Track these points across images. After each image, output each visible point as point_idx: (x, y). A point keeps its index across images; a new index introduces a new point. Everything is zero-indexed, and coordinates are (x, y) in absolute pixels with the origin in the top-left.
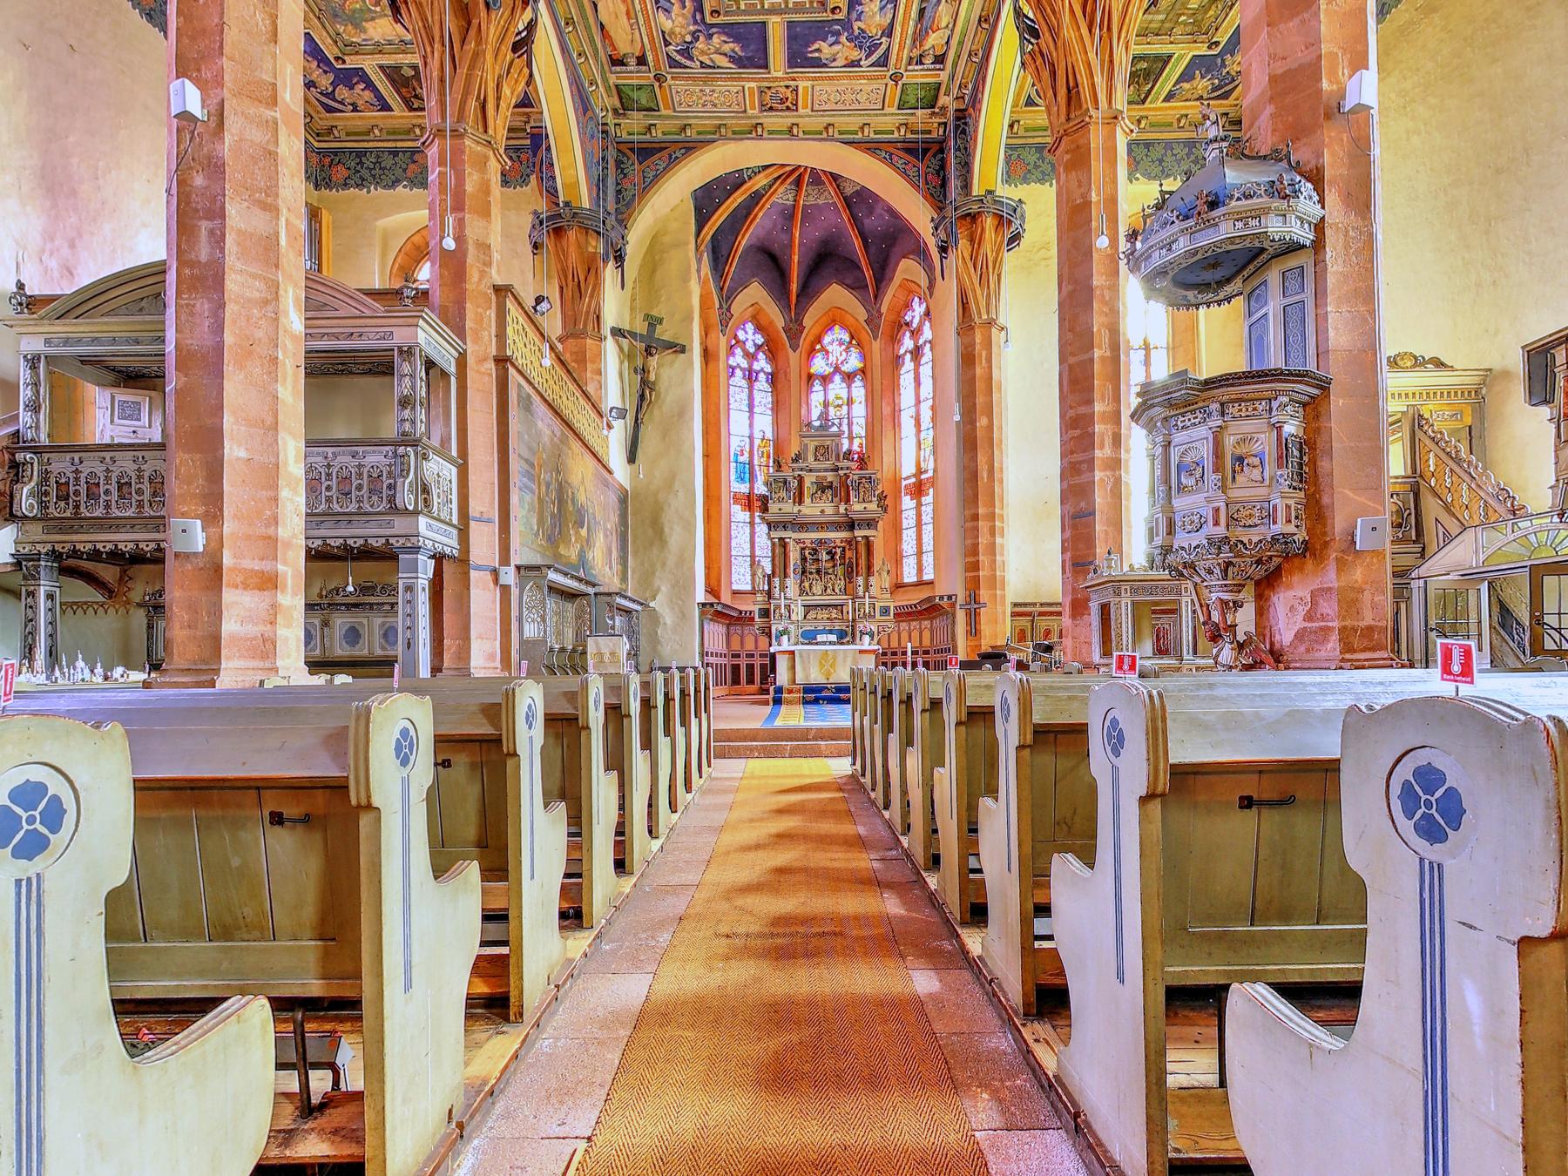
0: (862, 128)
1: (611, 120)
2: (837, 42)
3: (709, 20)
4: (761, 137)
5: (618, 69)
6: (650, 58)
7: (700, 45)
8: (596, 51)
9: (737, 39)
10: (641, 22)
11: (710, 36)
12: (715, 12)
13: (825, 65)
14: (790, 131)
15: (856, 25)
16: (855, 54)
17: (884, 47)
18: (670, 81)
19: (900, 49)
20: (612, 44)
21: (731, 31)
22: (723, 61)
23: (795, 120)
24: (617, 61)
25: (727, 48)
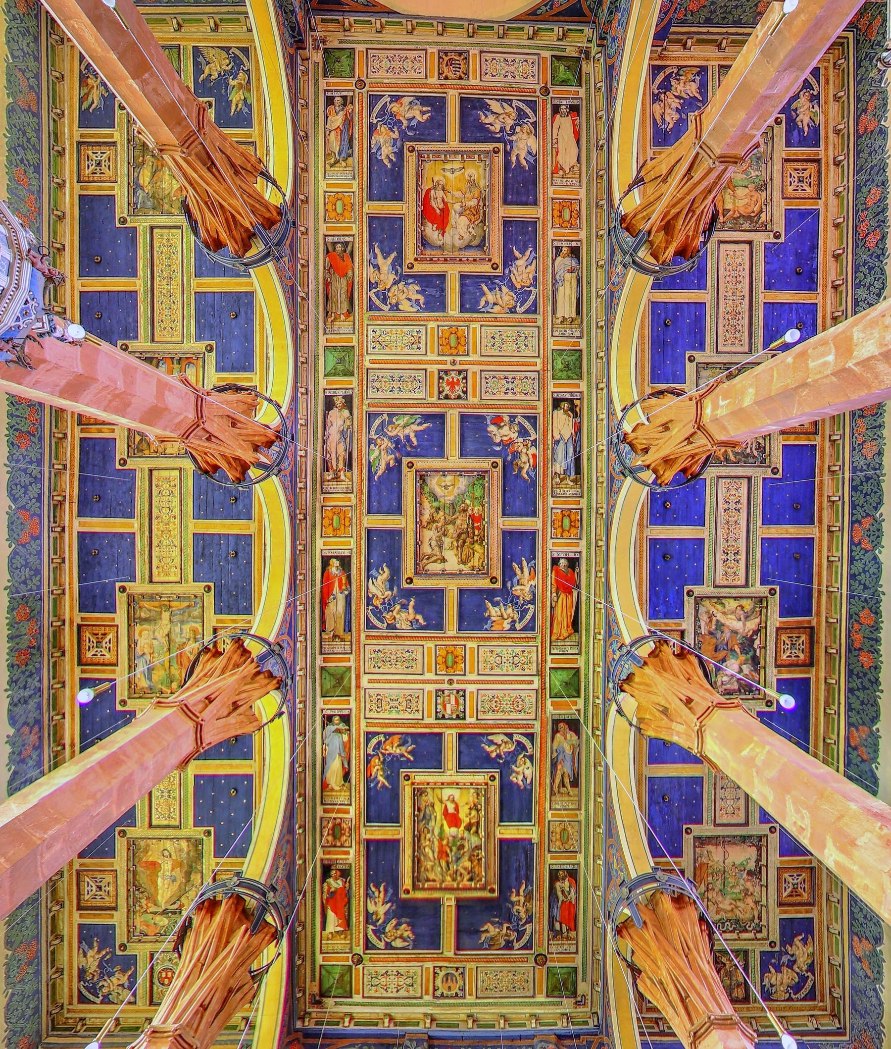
0: (382, 27)
1: (594, 50)
3: (501, 146)
4: (471, 21)
5: (575, 102)
6: (549, 112)
7: (510, 122)
8: (588, 121)
9: (482, 128)
11: (502, 130)
13: (417, 98)
14: (444, 27)
15: (396, 135)
16: (395, 107)
17: (374, 115)
18: (538, 87)
19: (360, 107)
20: (574, 125)
21: (486, 136)
22: (495, 106)
23: (440, 39)
24: (574, 109)
25: (491, 119)
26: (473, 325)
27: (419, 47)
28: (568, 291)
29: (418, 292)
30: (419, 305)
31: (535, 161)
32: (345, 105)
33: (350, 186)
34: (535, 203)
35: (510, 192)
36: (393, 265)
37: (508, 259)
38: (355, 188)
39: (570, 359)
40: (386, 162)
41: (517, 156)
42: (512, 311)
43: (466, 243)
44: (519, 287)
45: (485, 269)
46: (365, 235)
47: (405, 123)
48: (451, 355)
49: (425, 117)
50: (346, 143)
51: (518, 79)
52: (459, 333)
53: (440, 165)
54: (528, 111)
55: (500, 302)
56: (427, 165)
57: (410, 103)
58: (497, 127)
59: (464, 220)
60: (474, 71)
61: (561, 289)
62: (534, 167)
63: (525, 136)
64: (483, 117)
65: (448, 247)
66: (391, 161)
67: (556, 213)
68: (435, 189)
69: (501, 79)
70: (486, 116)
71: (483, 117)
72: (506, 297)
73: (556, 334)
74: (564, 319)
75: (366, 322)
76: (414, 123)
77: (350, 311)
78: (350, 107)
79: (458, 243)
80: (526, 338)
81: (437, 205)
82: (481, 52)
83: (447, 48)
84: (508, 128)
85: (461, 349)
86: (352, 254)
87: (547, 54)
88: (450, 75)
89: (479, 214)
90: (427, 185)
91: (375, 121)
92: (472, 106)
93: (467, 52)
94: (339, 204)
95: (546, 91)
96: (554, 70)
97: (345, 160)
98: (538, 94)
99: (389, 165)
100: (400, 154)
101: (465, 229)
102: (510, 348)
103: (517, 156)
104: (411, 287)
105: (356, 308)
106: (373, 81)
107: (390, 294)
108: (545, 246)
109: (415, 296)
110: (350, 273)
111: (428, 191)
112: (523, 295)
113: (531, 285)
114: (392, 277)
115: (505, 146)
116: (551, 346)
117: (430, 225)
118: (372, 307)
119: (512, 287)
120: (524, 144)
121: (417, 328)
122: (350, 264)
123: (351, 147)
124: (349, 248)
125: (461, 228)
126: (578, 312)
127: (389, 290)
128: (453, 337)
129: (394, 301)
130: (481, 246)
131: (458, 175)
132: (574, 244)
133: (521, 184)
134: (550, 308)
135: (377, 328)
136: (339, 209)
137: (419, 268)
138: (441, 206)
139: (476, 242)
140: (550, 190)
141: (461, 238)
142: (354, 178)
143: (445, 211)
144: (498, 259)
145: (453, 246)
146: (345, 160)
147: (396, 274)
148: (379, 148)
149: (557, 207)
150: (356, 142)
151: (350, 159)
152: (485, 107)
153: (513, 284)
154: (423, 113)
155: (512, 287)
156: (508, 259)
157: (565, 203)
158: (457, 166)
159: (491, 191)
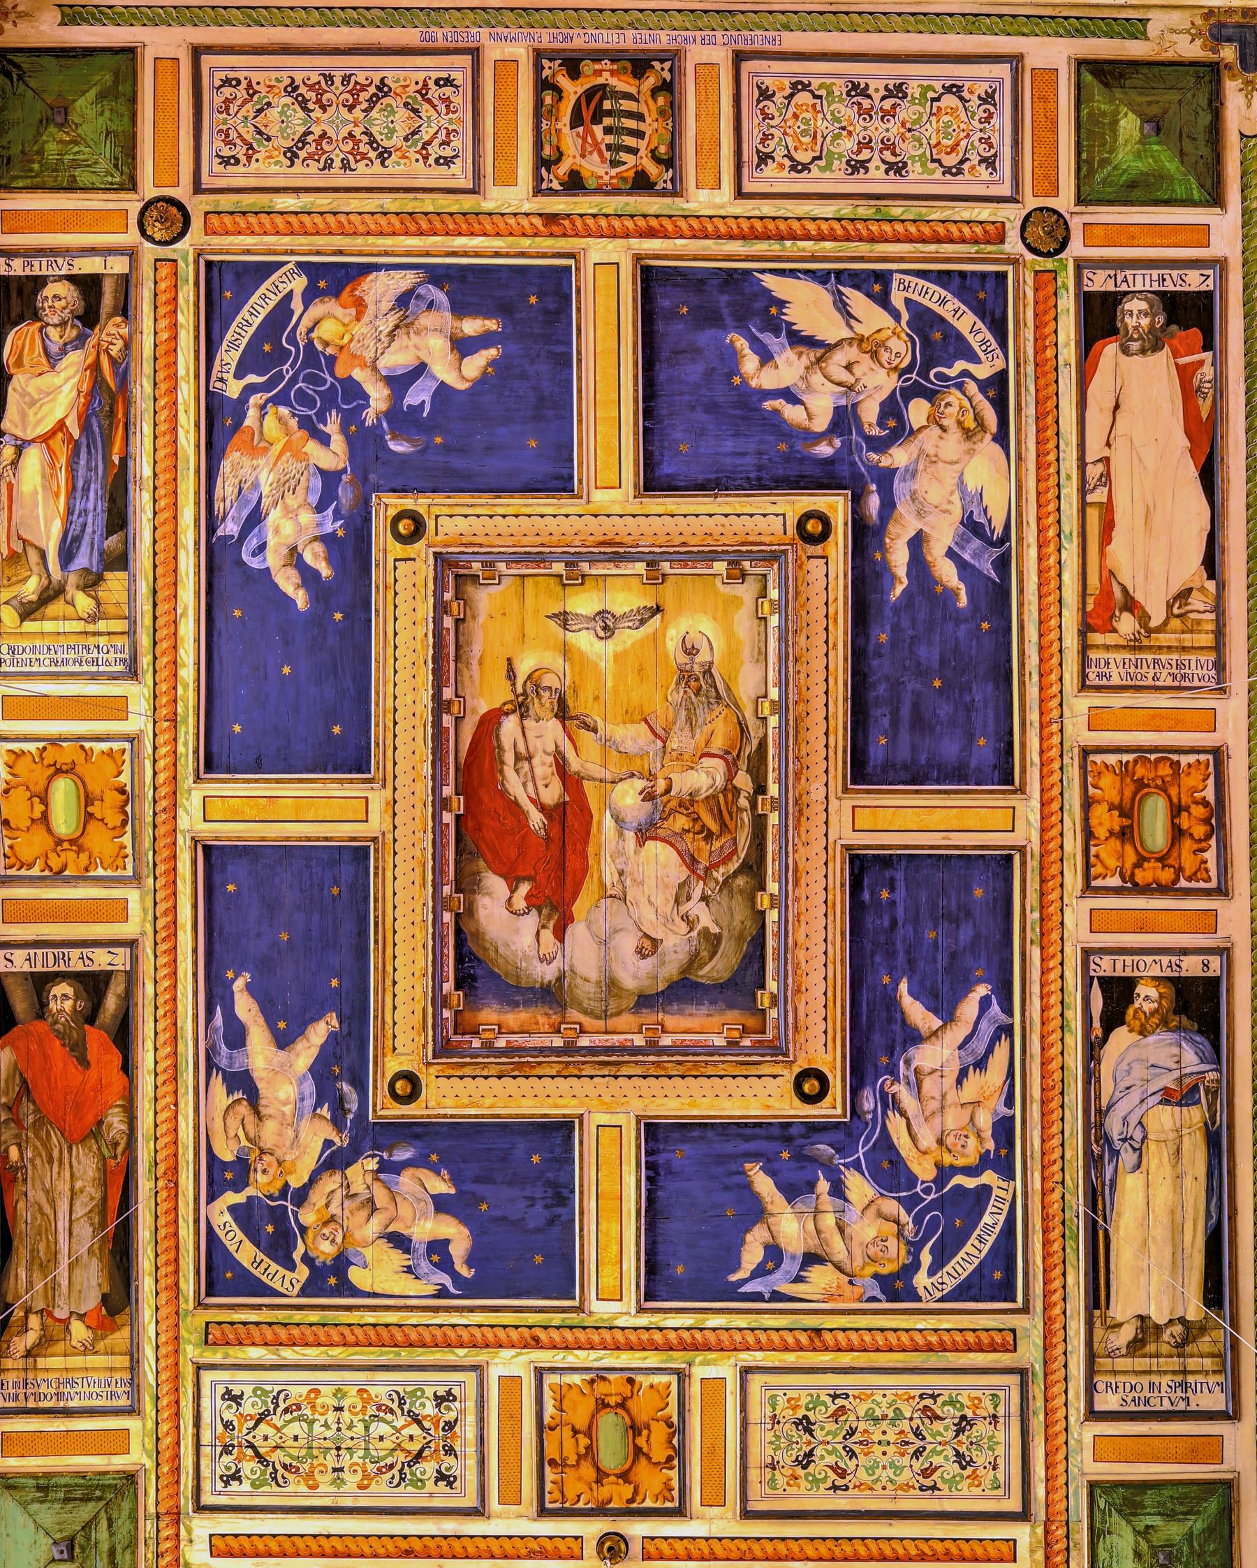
2: (399, 383)
3: (836, 505)
5: (1194, 281)
7: (879, 383)
9: (748, 408)
10: (1070, 491)
11: (844, 419)
12: (813, 532)
13: (436, 275)
15: (334, 456)
16: (328, 323)
17: (229, 356)
18: (1012, 215)
20: (1189, 393)
22: (807, 306)
25: (788, 368)
26: (705, 1368)
27: (442, 35)
28: (1163, 1194)
29: (441, 1205)
30: (445, 1264)
31: (1003, 564)
32: (89, 318)
33: (117, 708)
34: (1003, 773)
35: (881, 717)
36: (322, 1073)
37: (875, 1041)
38: (138, 722)
39: (1174, 1531)
40: (288, 582)
41: (917, 543)
42: (896, 1287)
43: (671, 970)
44: (924, 1171)
45: (766, 1098)
46: (185, 939)
47: (379, 397)
48: (601, 1511)
49: (475, 365)
50: (95, 503)
51: (920, 179)
52: (642, 1407)
53: (542, 598)
54: (966, 323)
55: (837, 1248)
56: (485, 599)
57: (403, 300)
58: (819, 408)
59: (660, 862)
60: (707, 149)
61: (1131, 1187)
62: (995, 596)
63: (952, 444)
64: (750, 363)
65: (587, 991)
66: (308, 576)
67: (1104, 820)
68: (521, 708)
69: (831, 178)
70: (766, 357)
71: (750, 363)
72: (864, 1222)
73: (1108, 1401)
74: (1147, 1330)
75: (191, 1351)
76: (418, 395)
77: (118, 1300)
78: (111, 330)
79: (634, 973)
80: (963, 1424)
81: (529, 788)
82: (739, 57)
83: (579, 40)
84: (870, 413)
85: (651, 1481)
86: (123, 1035)
87: (1054, 53)
88: (594, 168)
89: (731, 836)
90: (487, 693)
91: (234, 389)
92: (690, 310)
93: (673, 57)
94: (62, 791)
95: (1049, 233)
96: (1092, 134)
97: (91, 582)
98: (1013, 245)
99: (301, 599)
100: (352, 549)
101: (664, 900)
102: (884, 1474)
103: (917, 543)
104: (406, 1180)
105: (146, 1285)
106: (226, 202)
107: (308, 1217)
108: (1054, 992)
109: (426, 1228)
110: (116, 1122)
111: (491, 721)
112: (946, 1213)
113: (986, 1161)
114: (316, 1135)
115: (858, 500)
116: (1086, 1465)
117: (495, 884)
118: (220, 1275)
119: (890, 1172)
120: (949, 480)
121: (437, 1382)
122: (117, 1078)
123: (118, 519)
124: (111, 1003)
125: (644, 905)
126: (1216, 1286)
127: (301, 1196)
128: (610, 1426)
129: (326, 1250)
130: (742, 987)
131: (636, 637)
132: (1191, 966)
133: (930, 677)
134: (1076, 1280)
135: (244, 1382)
136: (64, 819)
137: (448, 1097)
138: (552, 793)
139: (717, 968)
140: (1070, 713)
141: (649, 946)
142: (132, 673)
143: (571, 818)
144: (825, 1050)
145: (611, 986)
146: (91, 582)
147: (337, 1122)
148: (255, 518)
149: (1108, 787)
150: (142, 503)
151: (115, 581)
152: (755, 309)
153: (897, 1161)
154: (463, 347)
155: (890, 1172)
156: (875, 1041)
157: (1147, 773)
158: (624, 600)
159: (794, 729)
